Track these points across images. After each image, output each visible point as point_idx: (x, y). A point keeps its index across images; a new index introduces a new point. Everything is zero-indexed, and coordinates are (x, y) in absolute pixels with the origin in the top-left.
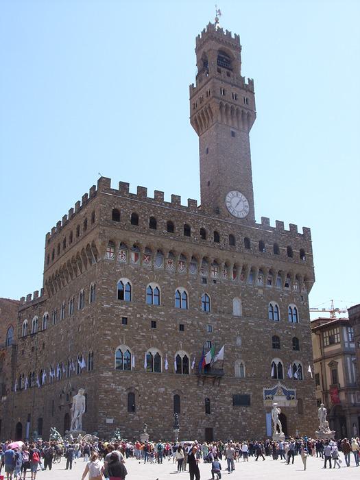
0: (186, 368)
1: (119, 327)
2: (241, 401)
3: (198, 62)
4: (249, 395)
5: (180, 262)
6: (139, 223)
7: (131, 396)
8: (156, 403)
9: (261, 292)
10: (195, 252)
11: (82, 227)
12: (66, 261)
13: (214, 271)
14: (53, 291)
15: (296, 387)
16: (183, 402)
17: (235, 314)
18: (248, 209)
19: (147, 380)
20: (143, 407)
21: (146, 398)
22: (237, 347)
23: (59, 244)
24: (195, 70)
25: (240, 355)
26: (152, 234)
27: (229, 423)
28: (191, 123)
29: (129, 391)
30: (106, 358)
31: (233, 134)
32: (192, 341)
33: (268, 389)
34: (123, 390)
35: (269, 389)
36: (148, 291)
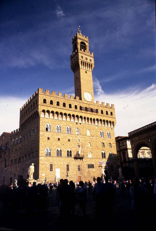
0: (71, 156)
2: (91, 166)
3: (73, 47)
6: (53, 104)
7: (51, 165)
9: (97, 127)
10: (73, 114)
11: (33, 106)
12: (27, 118)
14: (23, 129)
15: (110, 161)
16: (70, 167)
17: (87, 135)
18: (92, 98)
23: (25, 112)
24: (72, 50)
28: (71, 69)
31: (86, 72)
32: (73, 145)
36: (56, 128)
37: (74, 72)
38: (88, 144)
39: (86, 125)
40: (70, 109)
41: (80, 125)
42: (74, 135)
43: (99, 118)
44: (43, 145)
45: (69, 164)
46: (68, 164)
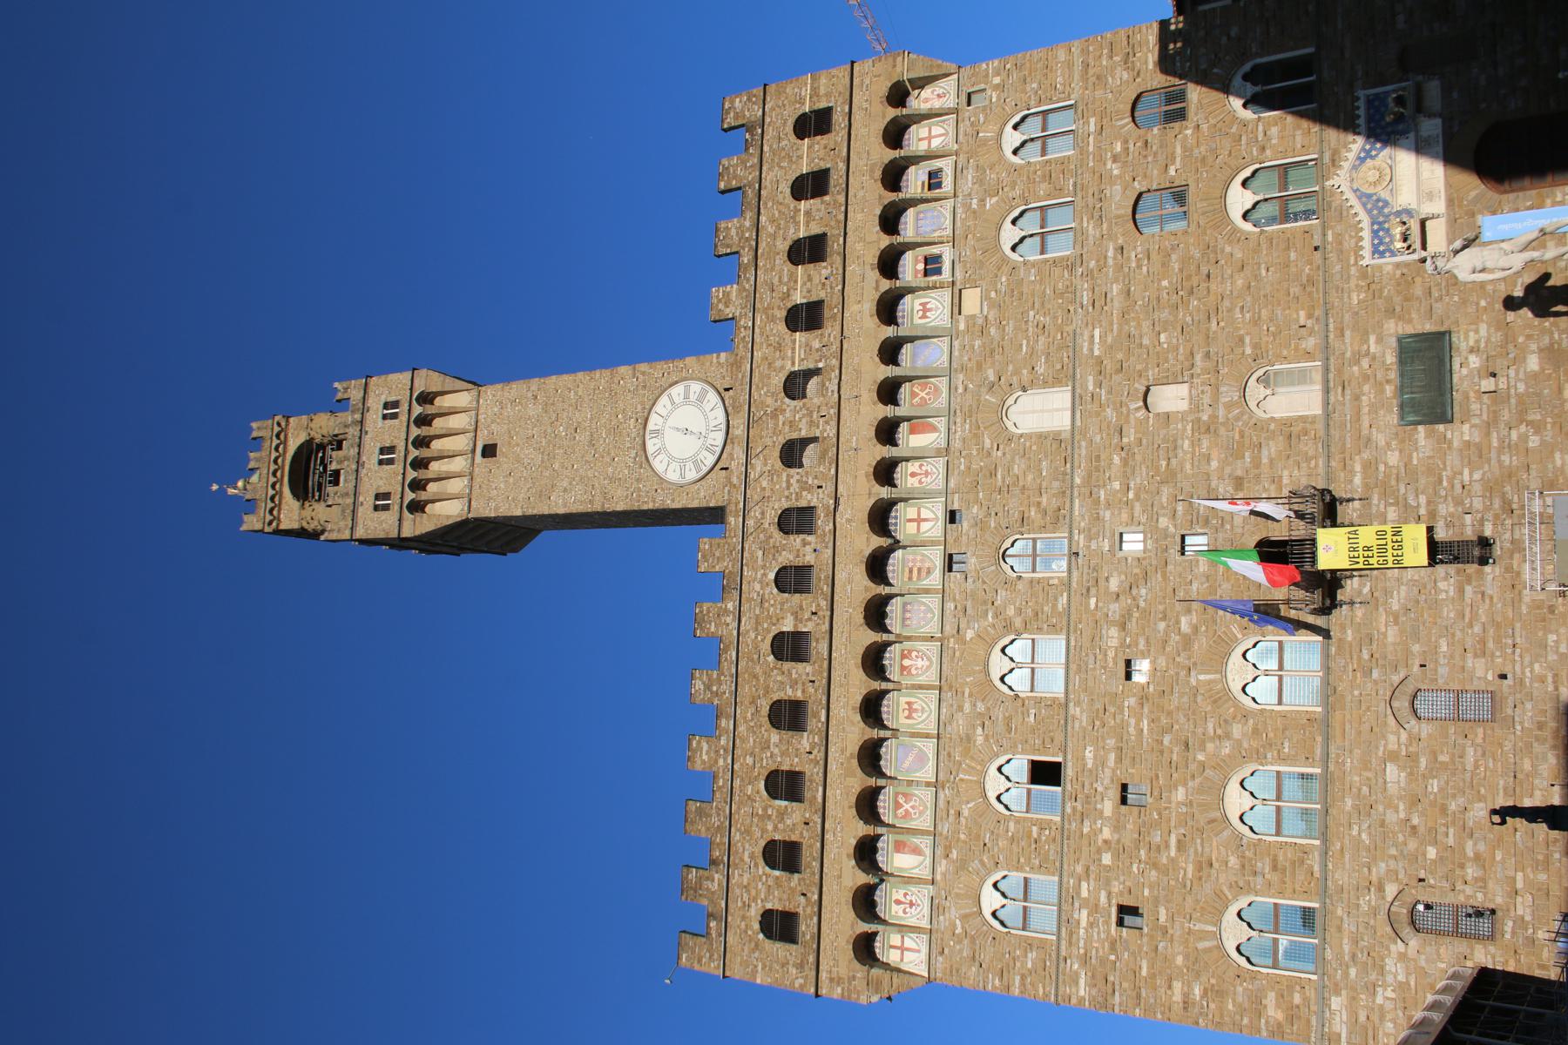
1: (1151, 937)
4: (1399, 340)
5: (903, 668)
6: (794, 838)
8: (1453, 806)
9: (972, 301)
10: (859, 617)
13: (919, 520)
18: (696, 387)
19: (1357, 841)
20: (1471, 872)
21: (1432, 853)
22: (1196, 406)
25: (1229, 393)
26: (820, 799)
27: (1534, 442)
28: (516, 550)
29: (1407, 931)
30: (1274, 1012)
31: (489, 451)
32: (1185, 624)
33: (1366, 243)
34: (1402, 957)
35: (1366, 234)
37: (539, 531)
38: (1168, 415)
39: (957, 444)
40: (819, 647)
41: (965, 524)
42: (1076, 599)
43: (868, 286)
44: (1197, 991)
45: (1410, 688)
46: (1402, 704)
